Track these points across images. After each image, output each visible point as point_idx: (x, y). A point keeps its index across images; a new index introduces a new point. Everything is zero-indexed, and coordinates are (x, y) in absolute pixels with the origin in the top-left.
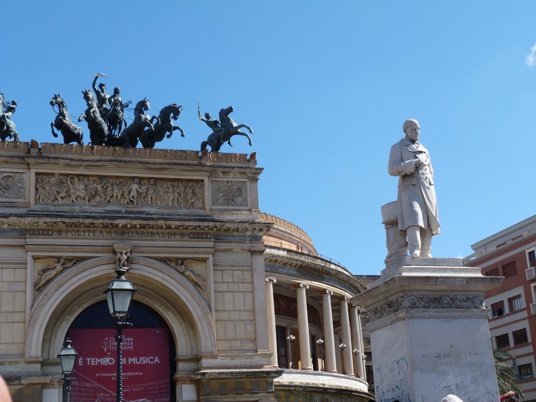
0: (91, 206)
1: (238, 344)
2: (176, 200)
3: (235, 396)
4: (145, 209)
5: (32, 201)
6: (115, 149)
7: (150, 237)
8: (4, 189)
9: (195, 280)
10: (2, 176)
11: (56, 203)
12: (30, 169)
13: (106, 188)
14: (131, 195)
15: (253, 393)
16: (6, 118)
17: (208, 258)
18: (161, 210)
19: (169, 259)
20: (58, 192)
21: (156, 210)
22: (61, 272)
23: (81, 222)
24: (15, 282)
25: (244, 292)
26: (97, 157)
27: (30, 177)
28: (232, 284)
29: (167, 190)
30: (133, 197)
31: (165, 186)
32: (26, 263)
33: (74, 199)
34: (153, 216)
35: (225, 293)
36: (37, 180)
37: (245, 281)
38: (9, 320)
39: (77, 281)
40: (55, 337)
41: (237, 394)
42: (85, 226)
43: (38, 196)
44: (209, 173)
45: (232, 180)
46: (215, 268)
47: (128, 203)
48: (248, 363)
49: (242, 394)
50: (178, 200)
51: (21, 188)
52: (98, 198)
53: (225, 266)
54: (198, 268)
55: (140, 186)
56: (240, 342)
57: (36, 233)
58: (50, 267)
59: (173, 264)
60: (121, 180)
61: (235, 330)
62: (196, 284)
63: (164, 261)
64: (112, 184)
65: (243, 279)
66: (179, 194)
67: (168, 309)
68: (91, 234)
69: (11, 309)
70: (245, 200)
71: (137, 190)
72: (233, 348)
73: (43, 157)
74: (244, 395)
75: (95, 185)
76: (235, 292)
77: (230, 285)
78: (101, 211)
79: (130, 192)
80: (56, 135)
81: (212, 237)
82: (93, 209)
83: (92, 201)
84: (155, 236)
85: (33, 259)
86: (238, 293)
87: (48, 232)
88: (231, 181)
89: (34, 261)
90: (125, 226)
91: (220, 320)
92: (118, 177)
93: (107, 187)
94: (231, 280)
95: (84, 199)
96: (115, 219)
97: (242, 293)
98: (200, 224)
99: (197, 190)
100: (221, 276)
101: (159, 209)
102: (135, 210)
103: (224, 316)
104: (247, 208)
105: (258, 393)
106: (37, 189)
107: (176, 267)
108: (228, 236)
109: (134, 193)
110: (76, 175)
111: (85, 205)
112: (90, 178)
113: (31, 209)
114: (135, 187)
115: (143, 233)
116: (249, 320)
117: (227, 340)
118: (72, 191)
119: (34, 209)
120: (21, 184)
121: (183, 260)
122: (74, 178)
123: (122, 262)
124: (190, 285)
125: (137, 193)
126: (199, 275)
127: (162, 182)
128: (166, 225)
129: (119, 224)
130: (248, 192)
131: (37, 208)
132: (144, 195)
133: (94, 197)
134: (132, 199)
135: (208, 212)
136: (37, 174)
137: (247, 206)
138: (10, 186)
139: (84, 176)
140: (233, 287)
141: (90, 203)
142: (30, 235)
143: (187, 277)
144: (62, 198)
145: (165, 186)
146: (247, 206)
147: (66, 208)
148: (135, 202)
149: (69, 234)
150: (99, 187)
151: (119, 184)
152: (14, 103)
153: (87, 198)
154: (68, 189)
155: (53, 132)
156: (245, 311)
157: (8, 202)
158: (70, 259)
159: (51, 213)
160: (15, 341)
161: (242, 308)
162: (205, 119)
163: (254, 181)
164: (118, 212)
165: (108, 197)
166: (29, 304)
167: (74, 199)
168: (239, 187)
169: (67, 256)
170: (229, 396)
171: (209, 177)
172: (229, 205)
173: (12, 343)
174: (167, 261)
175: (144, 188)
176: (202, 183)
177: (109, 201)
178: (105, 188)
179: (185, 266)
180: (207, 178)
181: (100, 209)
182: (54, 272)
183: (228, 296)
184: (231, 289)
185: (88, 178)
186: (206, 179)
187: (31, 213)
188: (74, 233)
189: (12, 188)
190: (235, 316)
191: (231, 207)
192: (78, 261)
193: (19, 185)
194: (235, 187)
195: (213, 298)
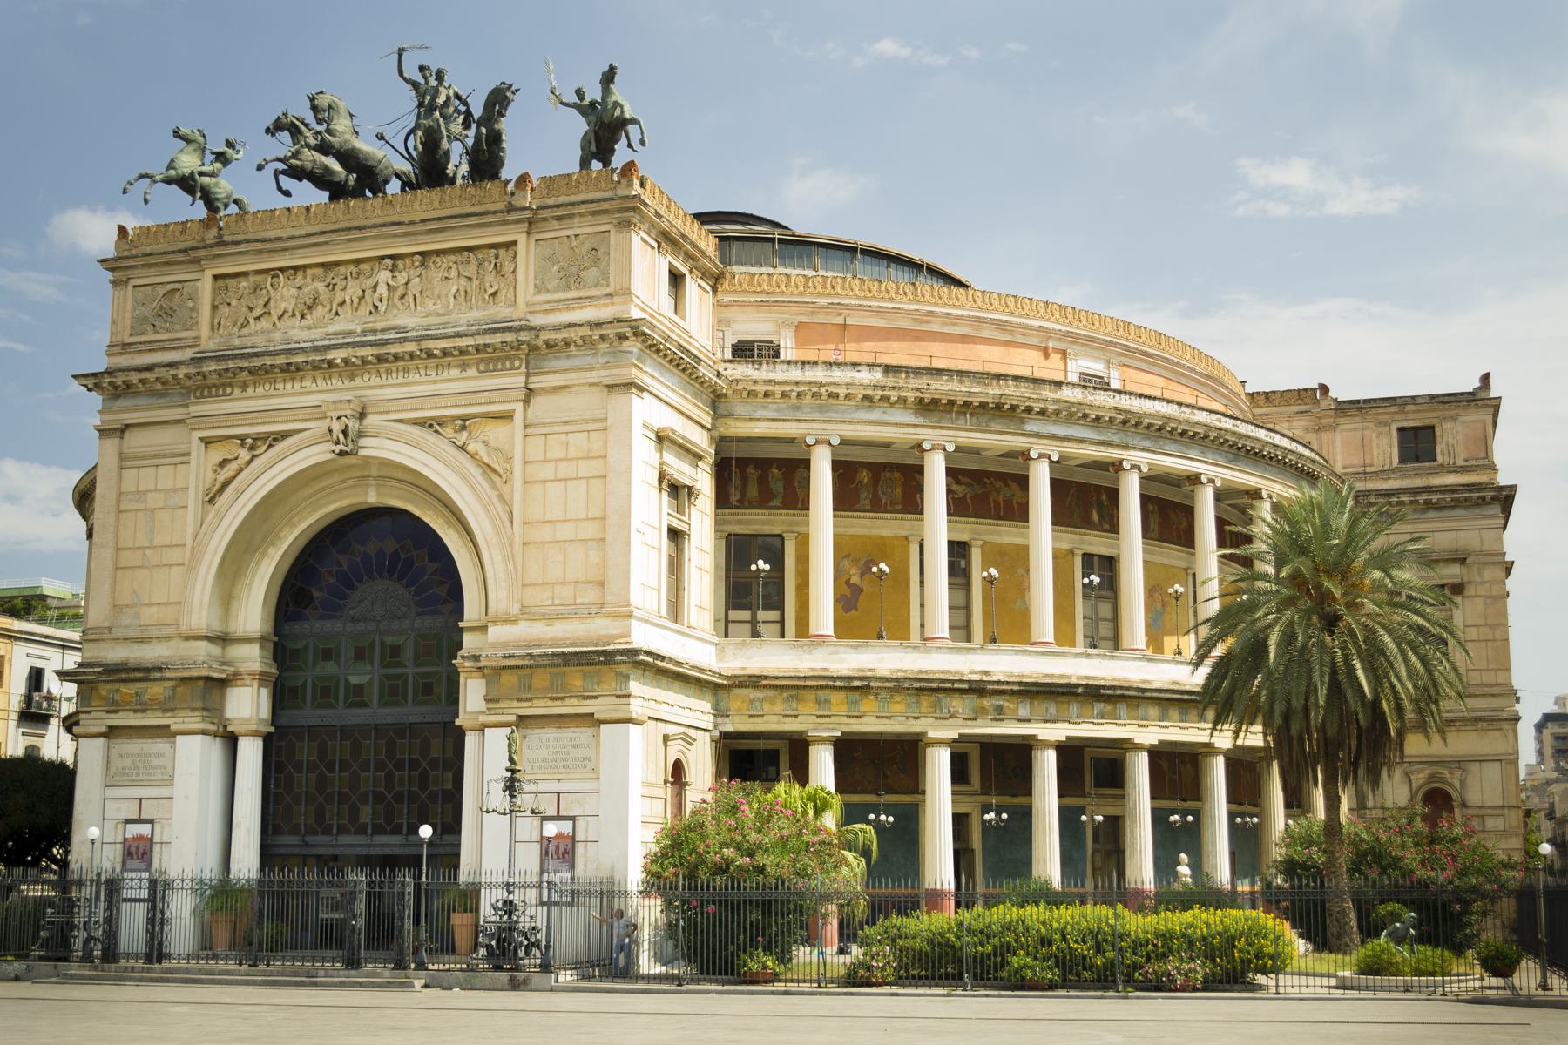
0: (302, 329)
1: (566, 593)
2: (463, 293)
4: (400, 322)
5: (205, 331)
6: (348, 206)
7: (401, 378)
8: (164, 315)
9: (486, 460)
10: (164, 291)
11: (245, 331)
12: (203, 270)
13: (334, 289)
14: (377, 295)
15: (585, 698)
16: (197, 177)
17: (514, 411)
18: (429, 318)
19: (441, 422)
20: (251, 309)
22: (249, 463)
23: (269, 363)
24: (175, 490)
25: (587, 478)
26: (316, 228)
27: (206, 286)
29: (446, 275)
30: (381, 301)
31: (444, 266)
32: (188, 454)
33: (276, 321)
34: (408, 334)
35: (548, 484)
36: (215, 291)
37: (593, 455)
38: (164, 562)
39: (269, 481)
40: (250, 590)
41: (552, 699)
42: (282, 371)
44: (526, 225)
45: (578, 231)
46: (529, 431)
47: (371, 313)
49: (562, 699)
50: (466, 292)
51: (192, 309)
52: (319, 311)
53: (551, 424)
54: (496, 433)
55: (397, 274)
56: (572, 587)
57: (206, 393)
58: (230, 457)
61: (565, 563)
62: (489, 469)
64: (346, 278)
65: (589, 451)
66: (470, 279)
67: (448, 523)
68: (297, 385)
69: (167, 542)
70: (605, 274)
71: (388, 285)
72: (556, 602)
73: (225, 244)
75: (315, 284)
77: (561, 465)
78: (313, 337)
79: (375, 287)
80: (287, 194)
81: (524, 365)
82: (305, 335)
83: (308, 317)
85: (203, 445)
86: (575, 482)
87: (224, 391)
88: (576, 236)
89: (206, 447)
90: (346, 361)
91: (535, 543)
92: (357, 262)
93: (334, 285)
94: (562, 455)
95: (294, 315)
96: (325, 350)
97: (584, 481)
98: (488, 339)
99: (507, 267)
101: (426, 316)
102: (379, 326)
103: (545, 533)
104: (608, 291)
106: (214, 307)
107: (455, 435)
108: (559, 358)
110: (282, 270)
111: (294, 327)
112: (309, 272)
113: (201, 349)
114: (384, 276)
115: (389, 372)
118: (272, 303)
119: (207, 348)
120: (194, 301)
122: (278, 276)
123: (335, 437)
124: (476, 472)
125: (389, 290)
126: (497, 450)
127: (438, 259)
128: (421, 350)
129: (334, 359)
130: (612, 255)
131: (211, 345)
132: (401, 291)
133: (310, 308)
134: (378, 304)
135: (519, 312)
136: (216, 277)
137: (608, 285)
138: (175, 308)
139: (296, 268)
140: (565, 470)
141: (304, 322)
142: (197, 398)
144: (258, 319)
145: (444, 266)
146: (608, 285)
147: (260, 341)
148: (382, 308)
149: (260, 390)
150: (320, 286)
151: (359, 274)
152: (229, 144)
154: (266, 299)
155: (280, 188)
156: (587, 519)
157: (169, 340)
158: (258, 438)
159: (230, 352)
160: (171, 600)
161: (583, 516)
162: (574, 99)
163: (624, 226)
164: (350, 333)
165: (334, 305)
166: (190, 530)
167: (276, 321)
168: (595, 246)
169: (257, 433)
171: (528, 233)
172: (569, 288)
173: (166, 604)
175: (402, 278)
176: (514, 248)
178: (331, 286)
179: (470, 434)
180: (525, 235)
181: (316, 334)
182: (234, 466)
183: (555, 489)
184: (561, 475)
185: (304, 272)
186: (522, 239)
187: (198, 355)
188: (267, 386)
189: (178, 312)
190: (566, 531)
191: (572, 294)
193: (190, 304)
194: (587, 247)
195: (517, 498)
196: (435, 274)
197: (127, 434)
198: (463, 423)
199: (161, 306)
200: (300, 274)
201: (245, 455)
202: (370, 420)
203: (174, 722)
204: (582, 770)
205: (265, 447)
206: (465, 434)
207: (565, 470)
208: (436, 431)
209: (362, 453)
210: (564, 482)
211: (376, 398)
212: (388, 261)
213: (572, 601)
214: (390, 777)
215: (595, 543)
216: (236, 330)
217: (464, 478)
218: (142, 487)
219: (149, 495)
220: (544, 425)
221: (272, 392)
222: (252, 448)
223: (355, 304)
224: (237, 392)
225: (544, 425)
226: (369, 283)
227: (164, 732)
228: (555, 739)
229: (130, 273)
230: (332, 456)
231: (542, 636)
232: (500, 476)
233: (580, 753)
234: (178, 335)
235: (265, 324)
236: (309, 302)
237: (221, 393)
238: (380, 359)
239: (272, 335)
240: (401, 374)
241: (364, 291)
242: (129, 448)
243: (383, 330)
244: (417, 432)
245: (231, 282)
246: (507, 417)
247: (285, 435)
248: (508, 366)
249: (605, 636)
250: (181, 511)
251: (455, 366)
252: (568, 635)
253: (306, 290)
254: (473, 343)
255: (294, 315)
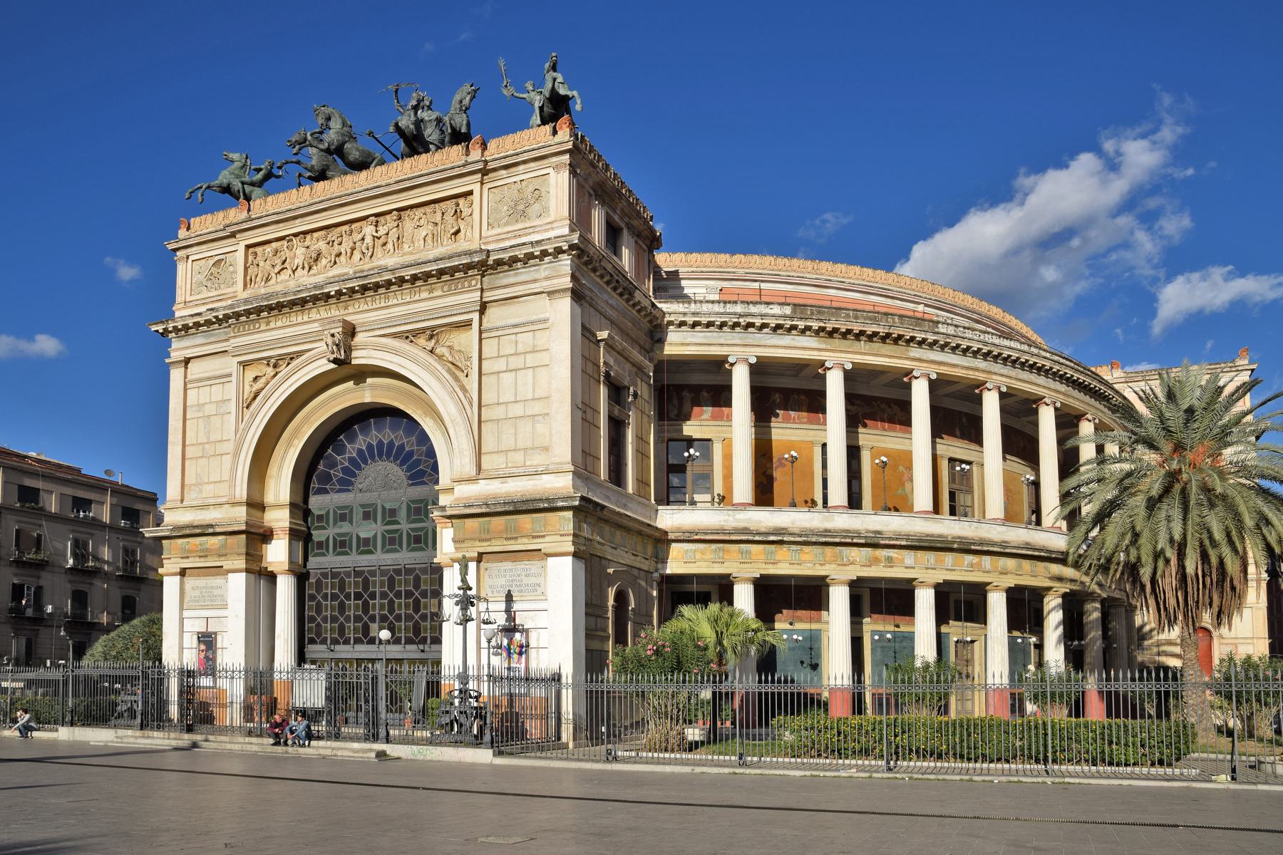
1: (518, 458)
3: (505, 542)
11: (270, 283)
13: (332, 246)
19: (417, 333)
21: (396, 259)
28: (515, 357)
35: (502, 375)
43: (248, 278)
48: (530, 487)
51: (232, 273)
52: (324, 262)
59: (422, 341)
60: (354, 226)
63: (410, 336)
64: (342, 236)
72: (510, 465)
74: (519, 541)
76: (519, 369)
77: (511, 359)
83: (315, 267)
84: (391, 300)
93: (333, 241)
100: (496, 348)
103: (499, 412)
105: (543, 536)
109: (368, 240)
110: (295, 235)
112: (316, 235)
116: (540, 415)
117: (502, 451)
121: (433, 328)
136: (248, 247)
139: (305, 233)
141: (311, 272)
143: (440, 357)
149: (279, 324)
150: (322, 245)
153: (306, 266)
158: (281, 357)
170: (494, 542)
174: (410, 336)
177: (335, 263)
182: (263, 380)
183: (507, 378)
188: (284, 320)
190: (517, 410)
192: (292, 359)
196: (408, 225)
197: (189, 365)
198: (432, 333)
199: (212, 274)
200: (308, 237)
201: (270, 371)
202: (360, 338)
203: (227, 564)
204: (533, 594)
205: (285, 365)
206: (433, 341)
207: (515, 362)
208: (412, 342)
209: (354, 362)
210: (513, 373)
211: (360, 321)
212: (373, 218)
213: (522, 464)
214: (391, 603)
215: (541, 417)
216: (263, 283)
217: (432, 373)
218: (201, 402)
219: (206, 406)
220: (497, 329)
221: (288, 323)
222: (275, 366)
223: (349, 254)
224: (263, 327)
225: (497, 329)
226: (357, 237)
227: (218, 570)
228: (511, 570)
229: (189, 251)
230: (332, 366)
231: (498, 491)
232: (463, 371)
233: (532, 580)
234: (223, 292)
235: (284, 276)
236: (314, 256)
237: (252, 328)
238: (364, 288)
239: (288, 283)
240: (383, 300)
241: (355, 243)
242: (192, 375)
243: (369, 270)
244: (396, 343)
245: (259, 250)
246: (468, 324)
247: (300, 354)
248: (466, 285)
249: (550, 489)
250: (228, 416)
251: (425, 290)
252: (519, 489)
253: (312, 248)
254: (436, 268)
255: (303, 268)
